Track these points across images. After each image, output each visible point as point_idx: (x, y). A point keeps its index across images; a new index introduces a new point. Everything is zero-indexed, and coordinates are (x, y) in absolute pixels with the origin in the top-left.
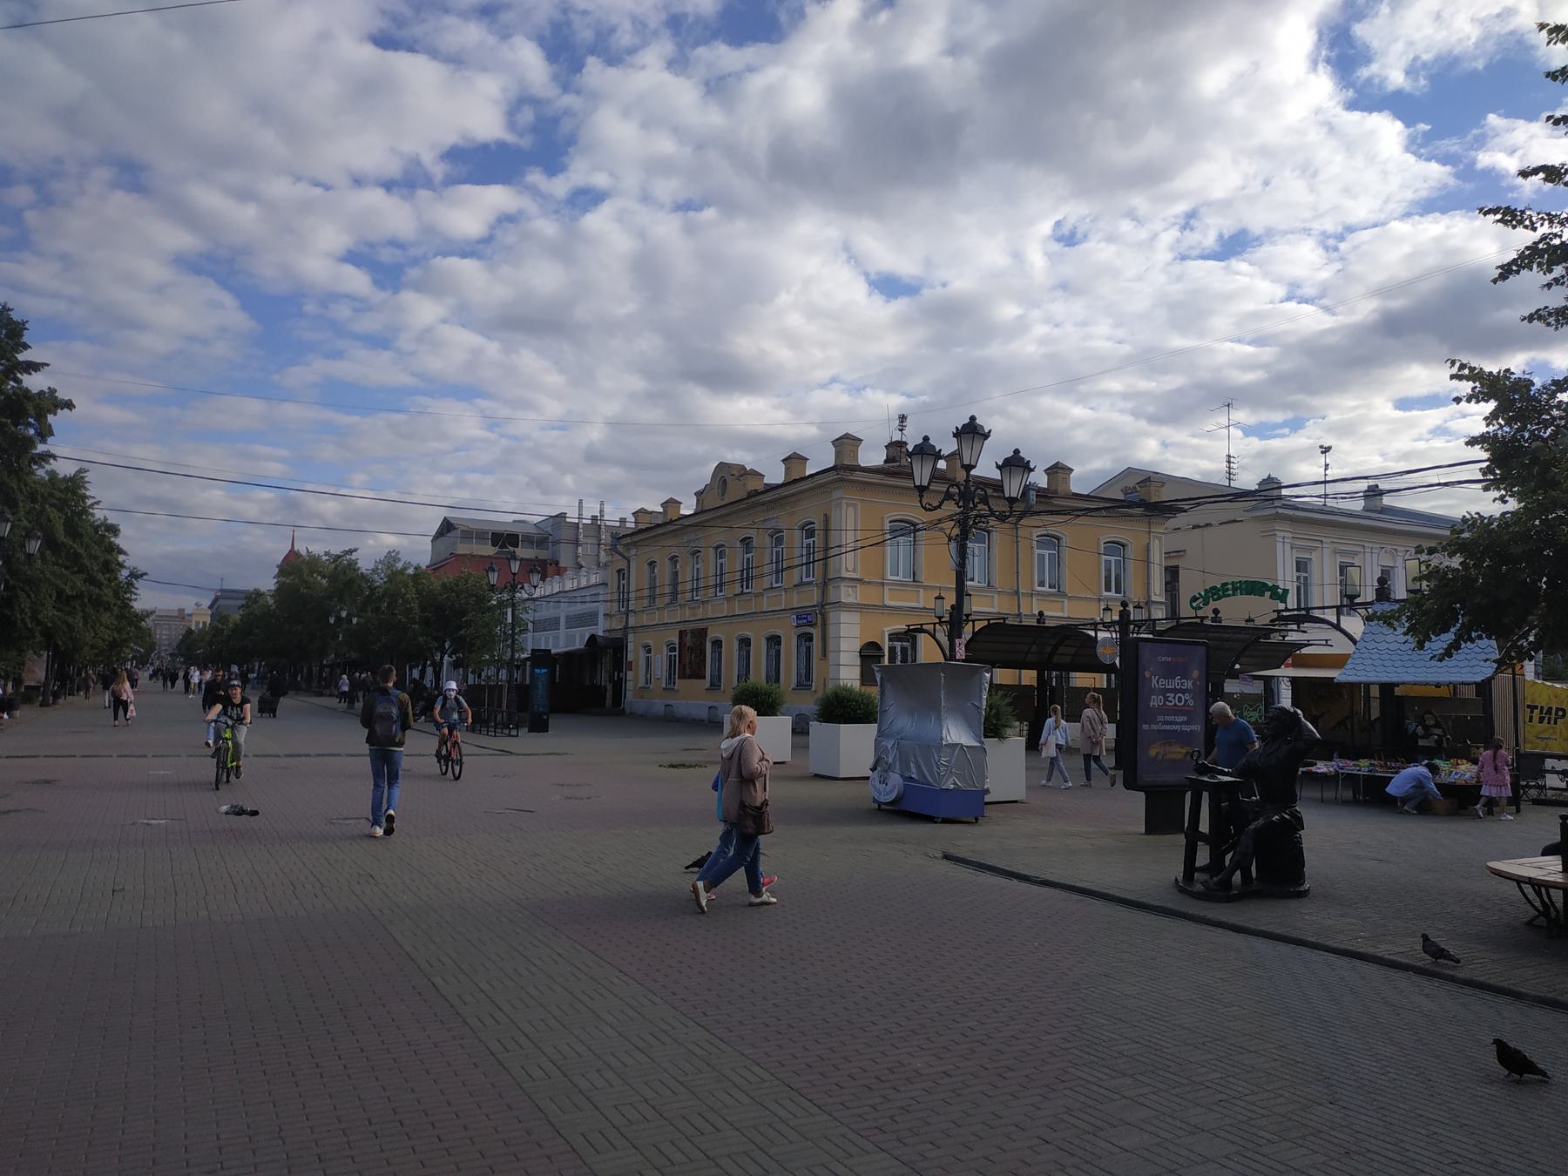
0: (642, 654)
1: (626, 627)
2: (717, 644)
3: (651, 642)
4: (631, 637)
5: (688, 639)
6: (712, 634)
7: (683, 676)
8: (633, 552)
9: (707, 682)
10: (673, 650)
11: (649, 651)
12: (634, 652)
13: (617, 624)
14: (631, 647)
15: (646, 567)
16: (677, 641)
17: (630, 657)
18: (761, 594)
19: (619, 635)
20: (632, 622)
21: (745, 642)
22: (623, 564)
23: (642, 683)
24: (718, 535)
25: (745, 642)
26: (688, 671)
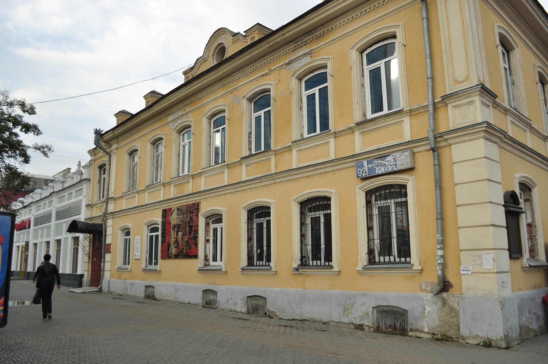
0: (121, 237)
1: (105, 216)
2: (217, 218)
3: (130, 225)
4: (110, 222)
5: (174, 219)
6: (206, 208)
7: (166, 255)
8: (114, 147)
9: (199, 262)
10: (156, 230)
11: (128, 234)
12: (113, 236)
13: (97, 212)
14: (109, 231)
15: (126, 156)
16: (158, 219)
17: (109, 240)
18: (289, 149)
19: (98, 221)
20: (111, 208)
21: (258, 213)
22: (106, 159)
23: (119, 262)
24: (214, 101)
25: (258, 213)
26: (173, 250)
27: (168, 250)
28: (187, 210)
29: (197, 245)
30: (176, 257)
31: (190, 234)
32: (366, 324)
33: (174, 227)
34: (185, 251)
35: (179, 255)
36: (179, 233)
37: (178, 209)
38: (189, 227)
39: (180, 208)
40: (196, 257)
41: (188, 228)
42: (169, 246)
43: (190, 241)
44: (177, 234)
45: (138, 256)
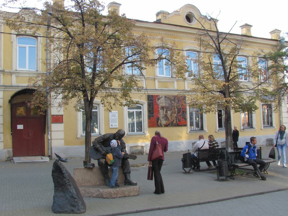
5: (162, 103)
27: (158, 122)
28: (175, 99)
29: (186, 119)
30: (166, 126)
31: (179, 113)
32: (264, 144)
33: (163, 108)
34: (175, 122)
35: (169, 124)
36: (168, 112)
37: (165, 97)
38: (177, 109)
39: (167, 97)
40: (185, 125)
41: (176, 109)
42: (158, 119)
43: (179, 117)
44: (166, 112)
45: (116, 125)
